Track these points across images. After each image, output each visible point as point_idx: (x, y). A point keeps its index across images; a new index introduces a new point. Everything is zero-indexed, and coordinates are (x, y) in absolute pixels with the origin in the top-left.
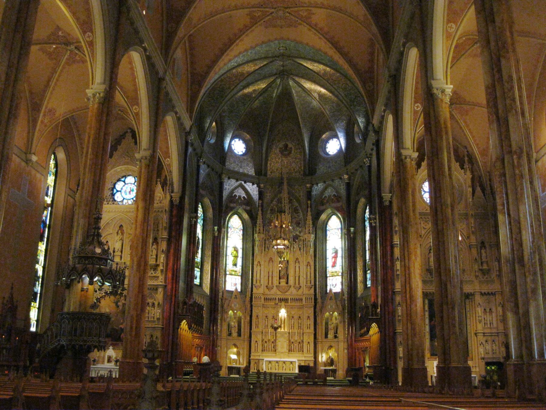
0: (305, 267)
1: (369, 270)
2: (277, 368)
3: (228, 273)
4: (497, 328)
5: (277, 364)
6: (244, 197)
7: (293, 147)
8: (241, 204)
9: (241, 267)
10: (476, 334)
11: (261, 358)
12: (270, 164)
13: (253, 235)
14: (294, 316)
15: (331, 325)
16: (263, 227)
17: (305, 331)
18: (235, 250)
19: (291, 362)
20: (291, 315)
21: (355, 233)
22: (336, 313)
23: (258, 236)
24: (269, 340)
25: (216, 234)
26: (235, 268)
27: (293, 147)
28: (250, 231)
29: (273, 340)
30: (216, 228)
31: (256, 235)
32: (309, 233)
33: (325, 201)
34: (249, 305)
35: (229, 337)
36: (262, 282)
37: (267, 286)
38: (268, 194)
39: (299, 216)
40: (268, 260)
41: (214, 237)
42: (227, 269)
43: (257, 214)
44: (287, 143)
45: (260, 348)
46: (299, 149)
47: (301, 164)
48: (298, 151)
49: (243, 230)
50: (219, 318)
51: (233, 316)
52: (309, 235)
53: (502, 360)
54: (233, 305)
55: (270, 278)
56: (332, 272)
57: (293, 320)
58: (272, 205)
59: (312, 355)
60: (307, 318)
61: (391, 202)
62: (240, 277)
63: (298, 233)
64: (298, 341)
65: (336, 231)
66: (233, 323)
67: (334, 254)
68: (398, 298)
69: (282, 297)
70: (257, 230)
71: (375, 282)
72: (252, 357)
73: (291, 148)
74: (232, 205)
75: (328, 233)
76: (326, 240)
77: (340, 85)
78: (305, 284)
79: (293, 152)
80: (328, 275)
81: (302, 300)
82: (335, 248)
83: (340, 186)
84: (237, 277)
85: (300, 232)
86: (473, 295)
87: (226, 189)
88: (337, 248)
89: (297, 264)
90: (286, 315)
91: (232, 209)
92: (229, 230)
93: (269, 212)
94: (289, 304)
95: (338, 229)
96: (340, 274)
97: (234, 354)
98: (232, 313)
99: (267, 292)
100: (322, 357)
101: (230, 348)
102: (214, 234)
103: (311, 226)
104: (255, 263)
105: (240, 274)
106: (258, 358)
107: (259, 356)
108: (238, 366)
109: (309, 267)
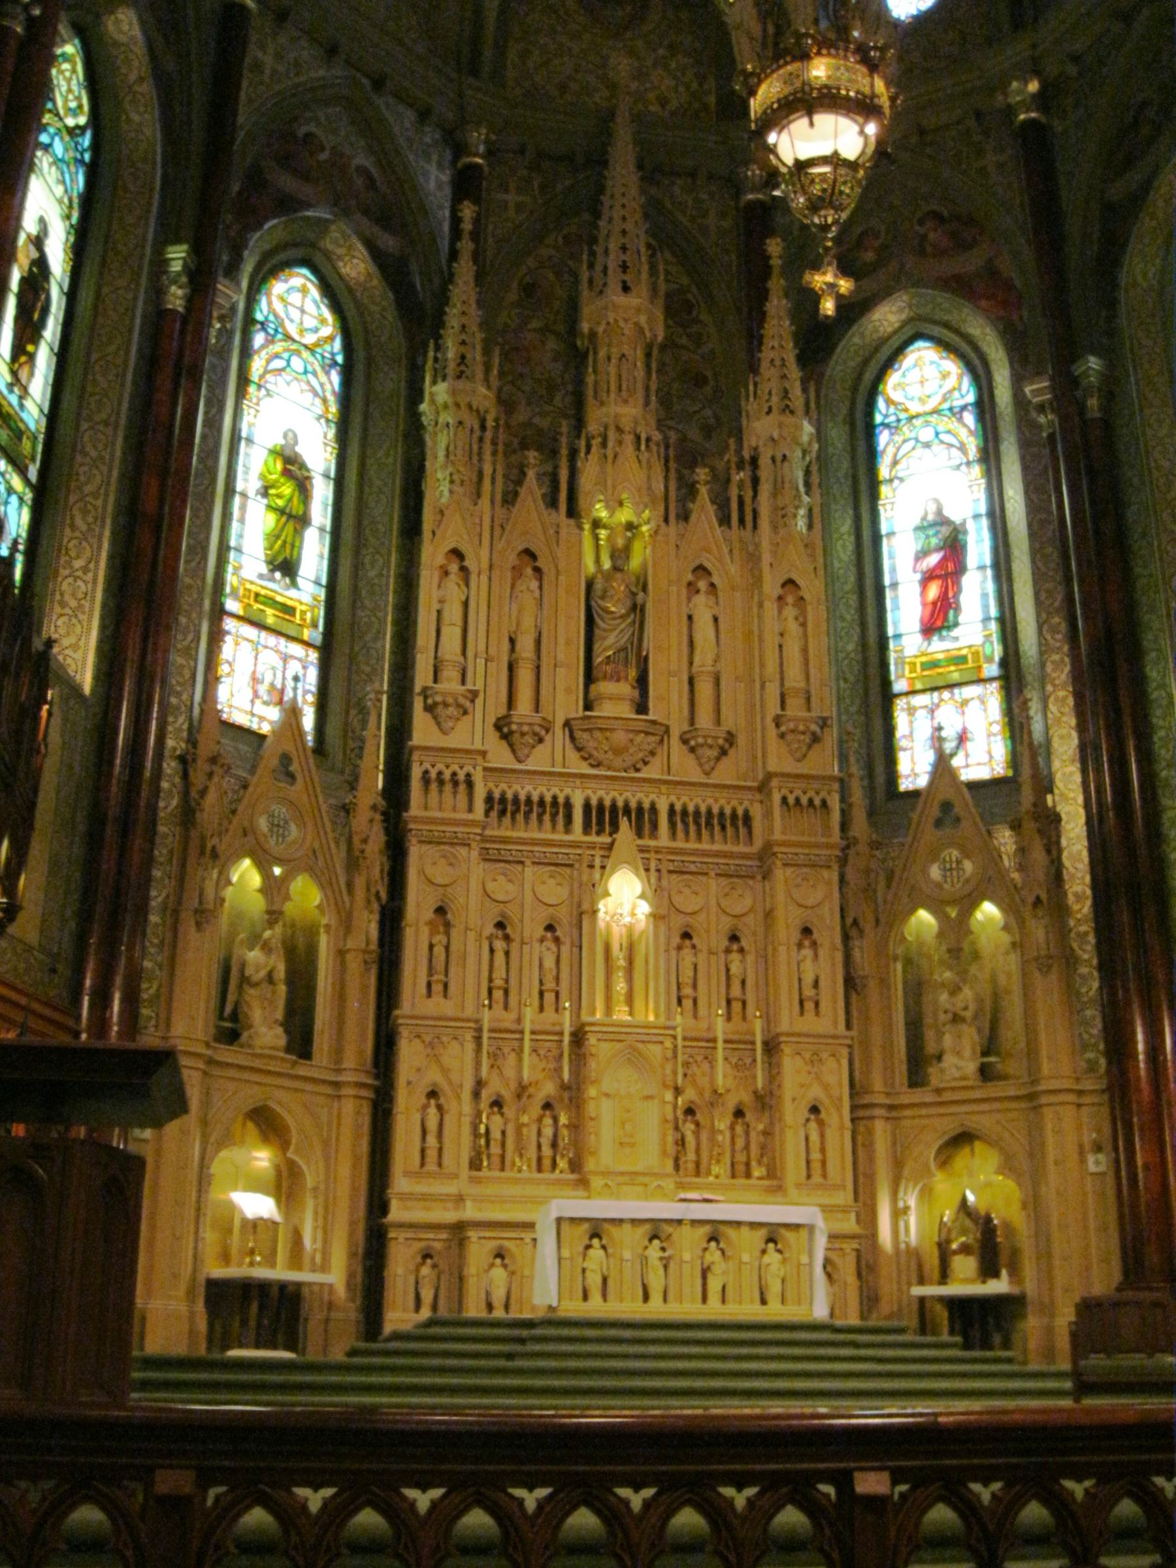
0: (770, 607)
2: (656, 1282)
3: (231, 605)
5: (654, 1252)
6: (362, 171)
8: (341, 204)
9: (322, 594)
11: (470, 1212)
12: (524, 55)
13: (415, 394)
14: (698, 923)
15: (955, 990)
16: (487, 352)
17: (784, 1026)
18: (286, 473)
19: (773, 1235)
20: (678, 922)
21: (1111, 388)
22: (988, 910)
23: (453, 392)
24: (522, 1091)
25: (176, 297)
26: (277, 587)
28: (391, 380)
29: (549, 1089)
30: (177, 256)
31: (438, 392)
32: (787, 410)
33: (869, 256)
34: (377, 839)
35: (226, 1054)
36: (476, 682)
37: (498, 727)
38: (512, 198)
39: (698, 340)
40: (512, 558)
41: (159, 316)
42: (231, 579)
43: (442, 298)
45: (459, 1146)
47: (702, 79)
48: (684, 15)
49: (347, 372)
50: (157, 897)
51: (256, 904)
52: (788, 419)
54: (263, 823)
55: (525, 677)
56: (934, 664)
57: (687, 953)
58: (531, 262)
59: (844, 1197)
60: (796, 936)
62: (313, 656)
63: (694, 434)
64: (731, 1103)
65: (946, 423)
66: (254, 956)
67: (934, 559)
69: (608, 794)
70: (451, 352)
72: (396, 1213)
74: (287, 182)
75: (883, 438)
76: (874, 485)
78: (773, 708)
80: (899, 686)
81: (747, 819)
82: (942, 521)
83: (980, 153)
84: (296, 649)
85: (707, 432)
87: (257, 67)
88: (955, 514)
89: (701, 600)
90: (644, 908)
91: (287, 205)
92: (259, 339)
93: (513, 296)
94: (663, 838)
95: (957, 413)
96: (992, 670)
97: (255, 1185)
98: (256, 880)
99: (501, 756)
100: (898, 1213)
101: (227, 1140)
102: (158, 292)
103: (795, 373)
104: (432, 554)
105: (315, 635)
106: (450, 1216)
107: (460, 1199)
108: (280, 1273)
109: (790, 612)
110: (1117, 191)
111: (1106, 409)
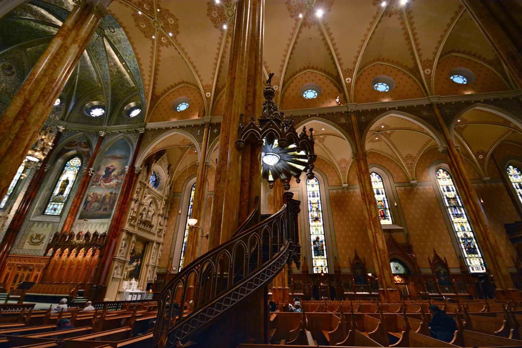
1: (52, 202)
4: (155, 263)
7: (16, 74)
10: (147, 266)
27: (16, 74)
44: (13, 67)
46: (20, 79)
48: (19, 79)
53: (153, 282)
61: (139, 173)
68: (124, 235)
71: (74, 214)
73: (14, 73)
77: (115, 80)
79: (14, 76)
86: (153, 242)
110: (66, 148)
111: (47, 171)
